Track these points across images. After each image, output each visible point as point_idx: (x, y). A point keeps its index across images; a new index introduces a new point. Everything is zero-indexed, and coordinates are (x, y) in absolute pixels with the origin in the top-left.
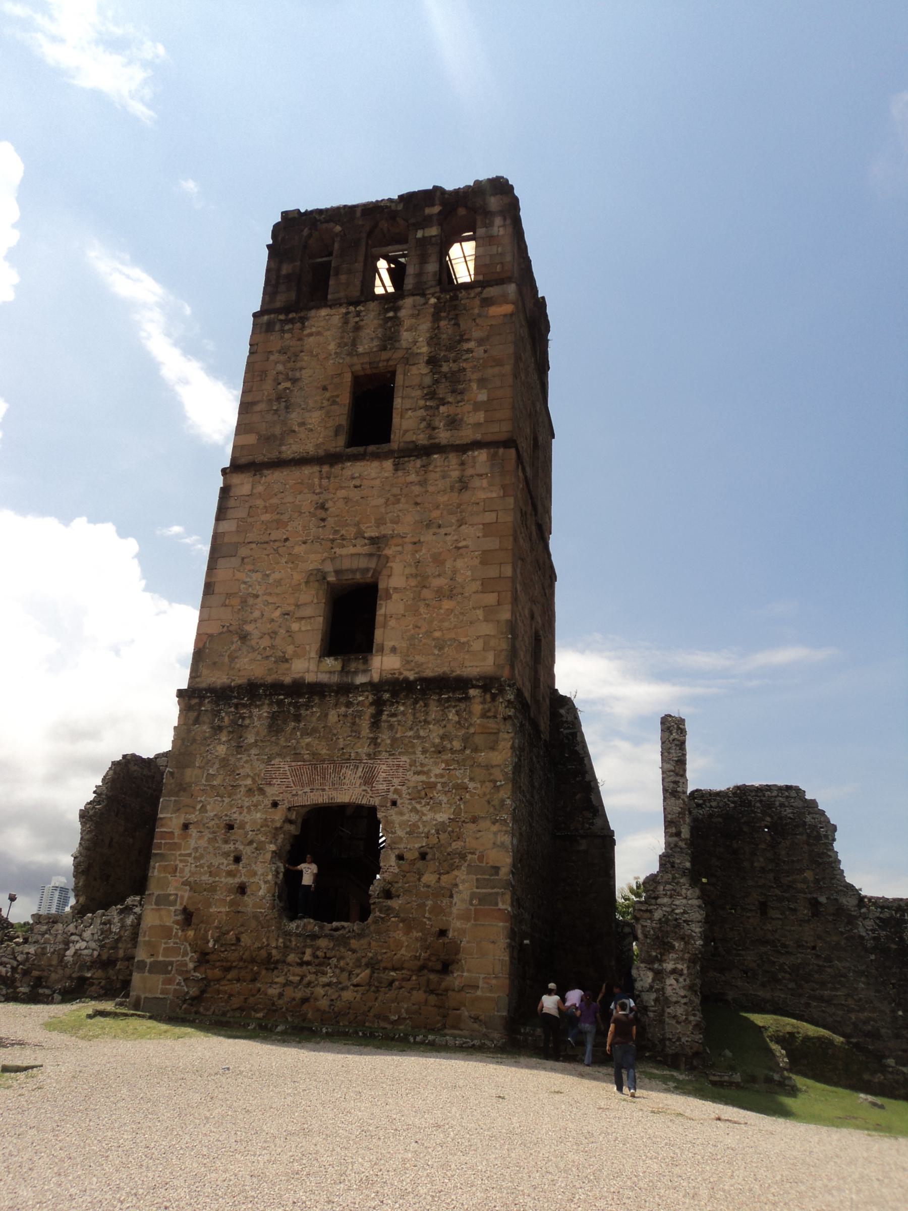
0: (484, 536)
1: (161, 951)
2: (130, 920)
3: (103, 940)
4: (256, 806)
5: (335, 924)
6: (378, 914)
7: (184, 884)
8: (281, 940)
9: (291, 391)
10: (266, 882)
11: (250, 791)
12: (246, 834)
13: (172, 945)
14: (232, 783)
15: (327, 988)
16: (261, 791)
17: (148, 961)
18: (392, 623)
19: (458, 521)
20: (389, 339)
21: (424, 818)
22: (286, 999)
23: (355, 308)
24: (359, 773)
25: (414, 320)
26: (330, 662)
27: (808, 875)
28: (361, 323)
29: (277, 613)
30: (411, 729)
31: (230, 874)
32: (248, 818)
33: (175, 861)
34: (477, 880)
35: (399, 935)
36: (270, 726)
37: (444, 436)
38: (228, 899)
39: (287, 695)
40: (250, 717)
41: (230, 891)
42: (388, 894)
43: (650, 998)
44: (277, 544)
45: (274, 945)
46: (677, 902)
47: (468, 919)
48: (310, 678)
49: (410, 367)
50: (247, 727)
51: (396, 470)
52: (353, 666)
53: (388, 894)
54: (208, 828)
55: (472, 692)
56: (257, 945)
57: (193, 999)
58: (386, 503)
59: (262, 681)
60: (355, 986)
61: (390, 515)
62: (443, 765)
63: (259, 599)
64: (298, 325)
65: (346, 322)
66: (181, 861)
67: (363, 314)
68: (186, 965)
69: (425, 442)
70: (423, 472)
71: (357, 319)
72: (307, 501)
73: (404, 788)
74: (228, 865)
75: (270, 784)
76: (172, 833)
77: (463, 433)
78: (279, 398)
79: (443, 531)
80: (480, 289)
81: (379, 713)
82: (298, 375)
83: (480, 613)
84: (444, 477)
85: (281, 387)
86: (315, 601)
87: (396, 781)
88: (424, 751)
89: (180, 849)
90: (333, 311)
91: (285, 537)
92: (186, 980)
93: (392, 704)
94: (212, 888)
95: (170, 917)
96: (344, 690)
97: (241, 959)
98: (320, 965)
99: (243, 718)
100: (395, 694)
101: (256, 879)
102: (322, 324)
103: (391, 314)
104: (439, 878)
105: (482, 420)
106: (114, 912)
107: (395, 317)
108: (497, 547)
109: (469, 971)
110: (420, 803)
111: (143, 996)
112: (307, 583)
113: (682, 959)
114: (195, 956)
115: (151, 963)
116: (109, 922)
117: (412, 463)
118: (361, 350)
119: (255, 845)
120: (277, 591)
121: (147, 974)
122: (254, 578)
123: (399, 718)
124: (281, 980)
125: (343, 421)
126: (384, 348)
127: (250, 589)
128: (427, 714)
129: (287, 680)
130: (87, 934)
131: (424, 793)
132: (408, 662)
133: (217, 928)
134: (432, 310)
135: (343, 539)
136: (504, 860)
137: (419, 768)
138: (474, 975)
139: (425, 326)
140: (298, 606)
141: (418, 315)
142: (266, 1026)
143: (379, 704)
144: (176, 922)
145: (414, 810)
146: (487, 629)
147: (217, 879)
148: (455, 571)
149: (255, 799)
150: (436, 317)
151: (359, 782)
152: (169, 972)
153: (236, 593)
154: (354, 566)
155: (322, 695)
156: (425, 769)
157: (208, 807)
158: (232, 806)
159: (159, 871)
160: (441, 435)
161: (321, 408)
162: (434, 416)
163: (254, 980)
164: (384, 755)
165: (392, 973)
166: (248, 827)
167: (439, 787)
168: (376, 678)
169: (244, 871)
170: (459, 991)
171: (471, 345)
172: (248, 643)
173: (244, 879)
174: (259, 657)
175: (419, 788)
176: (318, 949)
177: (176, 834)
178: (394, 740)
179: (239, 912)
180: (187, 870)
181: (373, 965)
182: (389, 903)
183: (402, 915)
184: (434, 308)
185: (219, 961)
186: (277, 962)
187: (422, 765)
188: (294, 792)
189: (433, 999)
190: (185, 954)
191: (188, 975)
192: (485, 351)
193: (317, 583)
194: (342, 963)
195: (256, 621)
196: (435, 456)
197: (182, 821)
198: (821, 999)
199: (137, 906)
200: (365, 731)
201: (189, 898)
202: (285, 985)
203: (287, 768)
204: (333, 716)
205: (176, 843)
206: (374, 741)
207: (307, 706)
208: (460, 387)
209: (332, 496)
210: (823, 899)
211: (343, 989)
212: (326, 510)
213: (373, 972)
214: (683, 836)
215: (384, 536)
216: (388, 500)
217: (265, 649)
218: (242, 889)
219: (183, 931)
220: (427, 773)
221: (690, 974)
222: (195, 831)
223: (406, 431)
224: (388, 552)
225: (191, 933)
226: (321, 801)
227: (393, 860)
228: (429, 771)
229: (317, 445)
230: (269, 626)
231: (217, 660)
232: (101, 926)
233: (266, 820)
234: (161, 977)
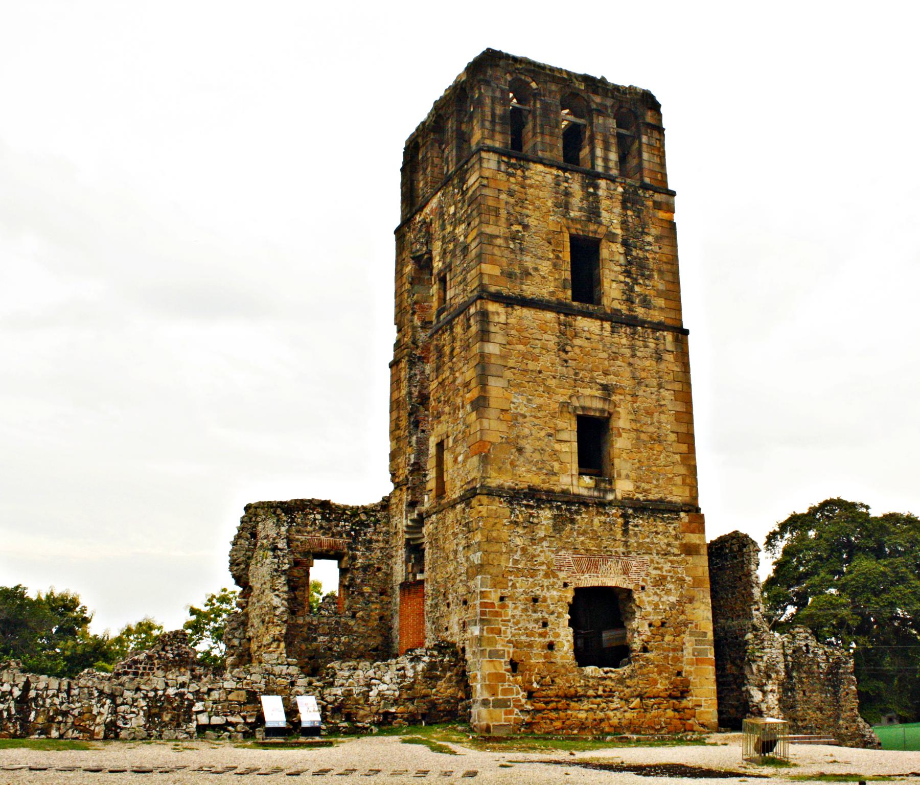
0: (676, 400)
1: (500, 692)
2: (420, 667)
3: (401, 683)
4: (553, 586)
5: (606, 669)
6: (641, 662)
7: (510, 642)
8: (582, 681)
9: (523, 236)
10: (568, 641)
11: (547, 575)
12: (548, 606)
13: (507, 687)
14: (533, 567)
15: (615, 712)
16: (556, 576)
17: (491, 699)
18: (624, 455)
19: (658, 385)
20: (593, 213)
21: (662, 599)
22: (590, 720)
23: (564, 173)
24: (620, 567)
25: (608, 202)
26: (587, 480)
28: (570, 189)
29: (543, 433)
30: (648, 537)
32: (548, 595)
33: (498, 624)
34: (696, 640)
35: (655, 676)
36: (554, 526)
37: (640, 312)
38: (543, 653)
39: (563, 502)
40: (538, 517)
41: (543, 648)
42: (645, 650)
43: (763, 707)
44: (534, 374)
45: (578, 685)
46: (773, 651)
47: (692, 664)
48: (575, 490)
49: (611, 244)
50: (537, 524)
51: (613, 332)
52: (603, 485)
53: (645, 650)
54: (520, 601)
55: (682, 514)
56: (568, 685)
57: (527, 724)
58: (609, 359)
59: (539, 488)
60: (631, 709)
61: (613, 368)
62: (669, 564)
63: (528, 419)
64: (519, 172)
65: (558, 185)
66: (503, 625)
67: (570, 181)
68: (520, 701)
69: (628, 313)
70: (630, 339)
71: (566, 185)
72: (551, 340)
73: (648, 578)
74: (539, 628)
75: (560, 570)
76: (493, 603)
77: (652, 312)
78: (513, 239)
79: (648, 389)
80: (651, 192)
81: (626, 523)
82: (526, 220)
83: (678, 457)
84: (646, 346)
85: (516, 227)
86: (569, 429)
87: (643, 574)
88: (657, 554)
89: (501, 616)
90: (547, 170)
91: (538, 369)
92: (522, 711)
93: (634, 518)
94: (530, 645)
95: (503, 666)
96: (602, 505)
97: (557, 696)
98: (609, 696)
99: (534, 517)
100: (635, 510)
101: (560, 640)
102: (540, 178)
103: (591, 190)
104: (674, 640)
105: (663, 306)
106: (404, 661)
107: (595, 195)
108: (685, 410)
109: (696, 696)
110: (659, 589)
111: (491, 725)
112: (561, 412)
113: (774, 683)
114: (526, 694)
115: (493, 700)
116: (403, 668)
117: (623, 330)
118: (572, 214)
119: (556, 615)
120: (539, 415)
121: (491, 708)
122: (521, 401)
123: (640, 528)
124: (586, 707)
125: (567, 275)
126: (589, 220)
127: (519, 410)
128: (656, 526)
129: (557, 489)
130: (387, 678)
132: (638, 487)
133: (537, 674)
134: (620, 198)
135: (583, 382)
136: (709, 628)
137: (656, 565)
138: (699, 698)
139: (618, 210)
140: (558, 431)
141: (611, 198)
142: (599, 738)
143: (624, 516)
144: (507, 671)
145: (656, 594)
146: (682, 470)
147: (533, 639)
148: (659, 422)
149: (552, 580)
150: (624, 208)
151: (621, 571)
152: (509, 706)
153: (508, 410)
154: (594, 406)
155: (586, 505)
156: (660, 566)
157: (517, 585)
159: (488, 633)
160: (637, 310)
161: (549, 259)
162: (632, 292)
163: (566, 709)
164: (634, 554)
165: (653, 700)
166: (549, 602)
167: (669, 578)
168: (619, 497)
169: (551, 633)
170: (692, 708)
171: (649, 239)
172: (524, 454)
173: (552, 639)
174: (534, 469)
175: (658, 579)
176: (606, 686)
177: (496, 604)
178: (640, 545)
179: (552, 662)
180: (509, 632)
181: (641, 696)
182: (647, 655)
183: (656, 663)
184: (622, 196)
185: (543, 697)
186: (581, 696)
187: (658, 563)
188: (578, 577)
189: (676, 713)
190: (518, 693)
191: (523, 708)
192: (660, 249)
193: (568, 415)
194: (622, 694)
195: (527, 437)
196: (639, 328)
197: (499, 595)
199: (424, 656)
200: (619, 536)
201: (513, 653)
202: (587, 711)
203: (571, 559)
204: (596, 520)
205: (497, 612)
206: (626, 544)
207: (578, 512)
208: (647, 273)
209: (569, 342)
211: (625, 711)
212: (567, 352)
213: (641, 700)
214: (761, 610)
215: (612, 384)
216: (610, 355)
217: (537, 462)
218: (551, 646)
219: (513, 676)
220: (660, 569)
221: (779, 692)
222: (511, 602)
223: (613, 299)
224: (613, 398)
225: (519, 678)
226: (596, 584)
227: (646, 627)
228: (662, 567)
229: (550, 292)
230: (538, 444)
231: (501, 465)
232: (397, 672)
233: (560, 596)
234: (503, 710)
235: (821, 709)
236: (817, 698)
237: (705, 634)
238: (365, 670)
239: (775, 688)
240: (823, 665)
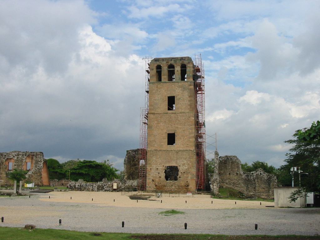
11: (159, 164)
16: (161, 164)
27: (236, 169)
31: (158, 175)
43: (212, 188)
53: (180, 177)
94: (156, 177)
124: (167, 188)
130: (135, 182)
131: (184, 164)
149: (161, 165)
158: (157, 166)
197: (150, 168)
198: (237, 187)
210: (238, 173)
220: (184, 162)
235: (264, 189)
236: (263, 186)
237: (194, 174)
238: (131, 181)
239: (216, 185)
240: (265, 178)
